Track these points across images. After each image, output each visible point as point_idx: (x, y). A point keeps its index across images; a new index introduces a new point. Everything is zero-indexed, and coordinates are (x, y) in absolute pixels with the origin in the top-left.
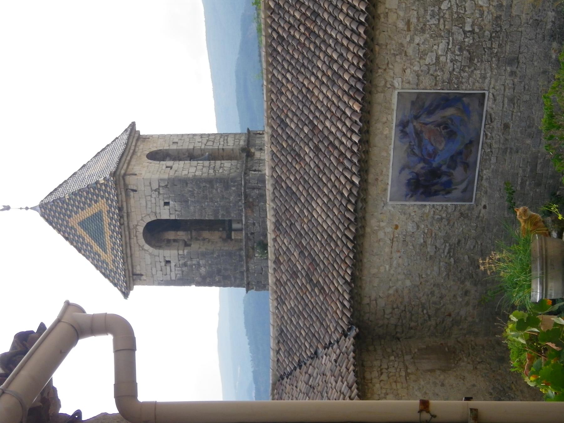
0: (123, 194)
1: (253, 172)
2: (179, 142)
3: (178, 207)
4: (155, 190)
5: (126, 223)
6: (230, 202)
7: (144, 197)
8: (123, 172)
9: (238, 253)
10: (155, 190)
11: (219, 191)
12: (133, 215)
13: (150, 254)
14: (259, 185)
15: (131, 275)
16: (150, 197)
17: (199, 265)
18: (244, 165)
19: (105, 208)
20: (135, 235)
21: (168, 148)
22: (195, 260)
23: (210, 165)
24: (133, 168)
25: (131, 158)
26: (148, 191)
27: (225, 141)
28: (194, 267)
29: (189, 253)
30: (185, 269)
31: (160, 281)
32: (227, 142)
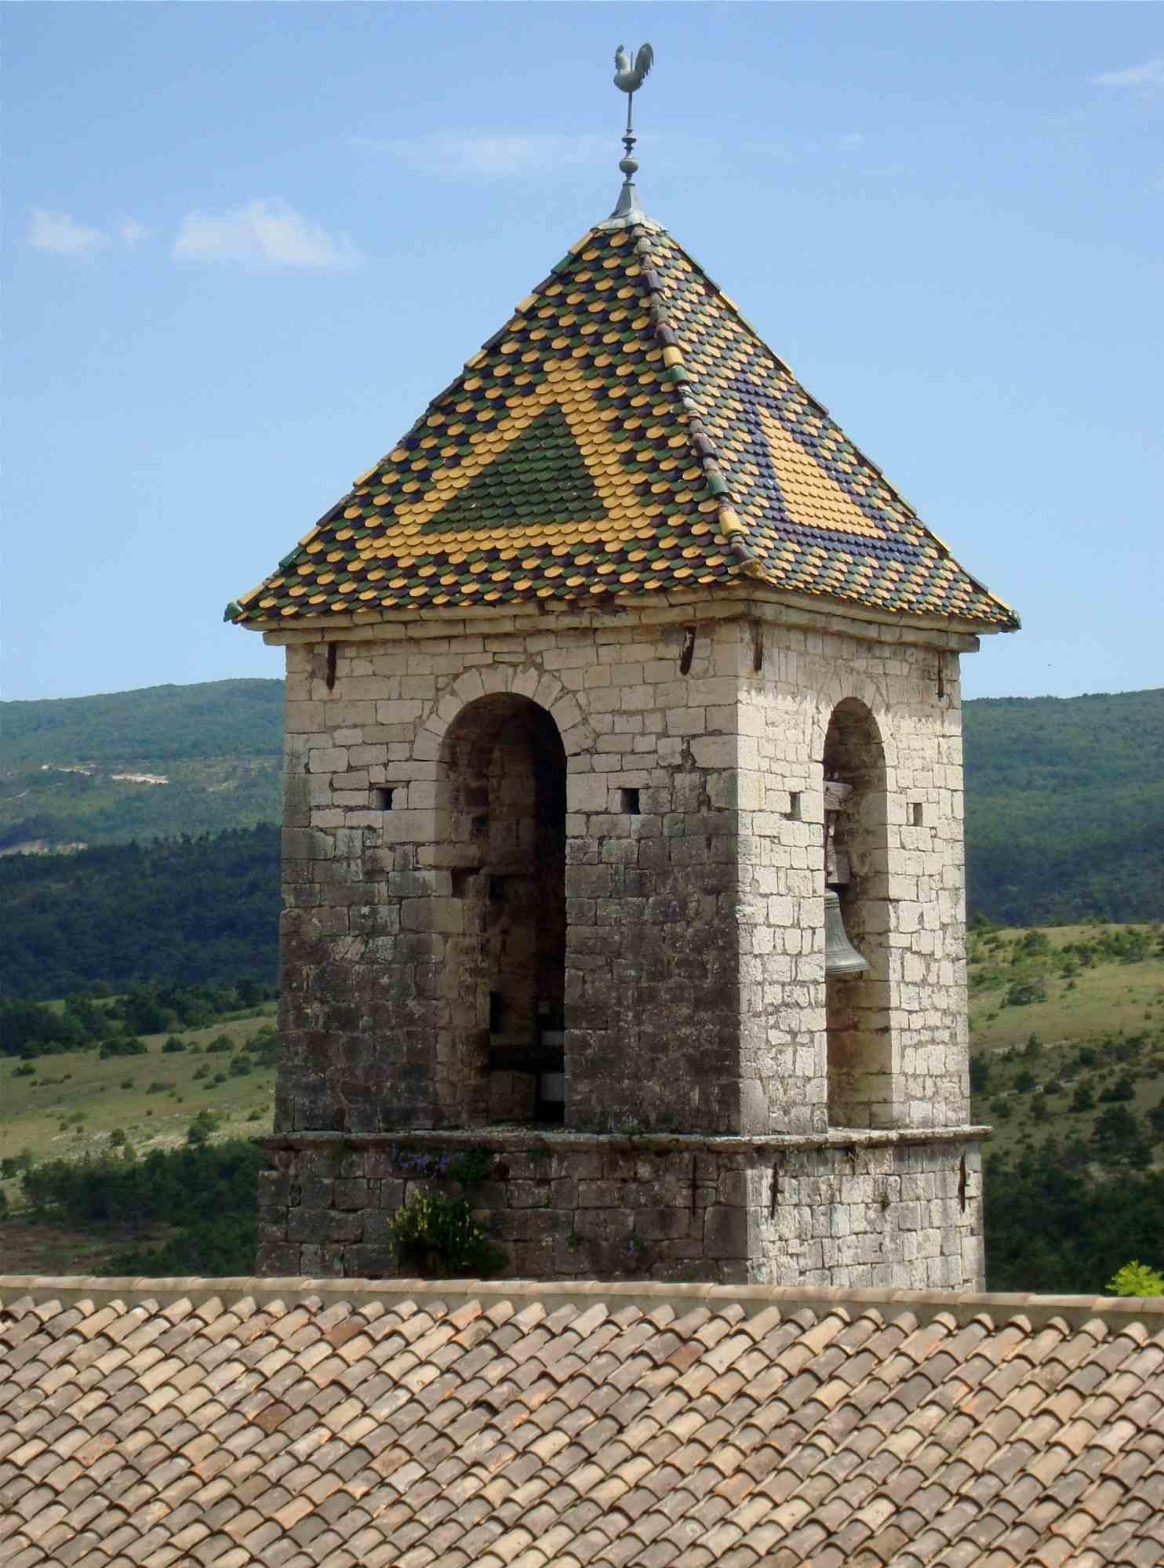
0: (674, 616)
1: (767, 1182)
2: (922, 832)
3: (615, 848)
4: (687, 754)
5: (550, 622)
6: (636, 1077)
7: (661, 702)
8: (769, 612)
9: (420, 1105)
10: (687, 754)
11: (685, 1031)
12: (583, 653)
13: (419, 723)
14: (710, 1209)
15: (330, 637)
16: (659, 728)
17: (371, 932)
18: (800, 1139)
19: (612, 532)
20: (498, 658)
21: (891, 784)
22: (395, 916)
23: (803, 984)
24: (788, 648)
25: (840, 635)
26: (682, 721)
27: (926, 1036)
28: (365, 910)
29: (424, 889)
30: (357, 868)
31: (304, 760)
32: (919, 1045)
